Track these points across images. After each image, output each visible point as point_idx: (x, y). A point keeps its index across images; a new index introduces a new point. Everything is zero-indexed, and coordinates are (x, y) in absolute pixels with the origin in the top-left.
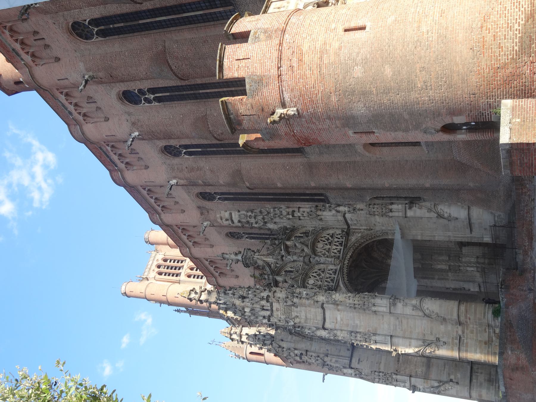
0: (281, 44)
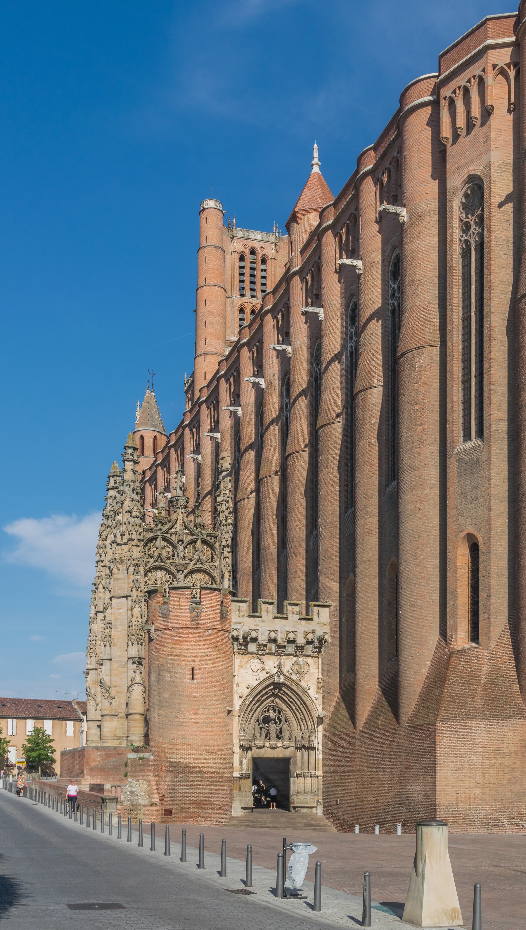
0: (187, 628)
